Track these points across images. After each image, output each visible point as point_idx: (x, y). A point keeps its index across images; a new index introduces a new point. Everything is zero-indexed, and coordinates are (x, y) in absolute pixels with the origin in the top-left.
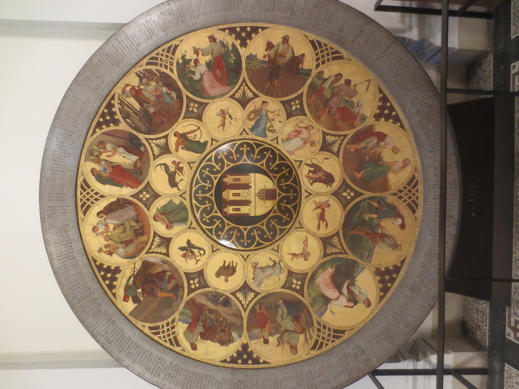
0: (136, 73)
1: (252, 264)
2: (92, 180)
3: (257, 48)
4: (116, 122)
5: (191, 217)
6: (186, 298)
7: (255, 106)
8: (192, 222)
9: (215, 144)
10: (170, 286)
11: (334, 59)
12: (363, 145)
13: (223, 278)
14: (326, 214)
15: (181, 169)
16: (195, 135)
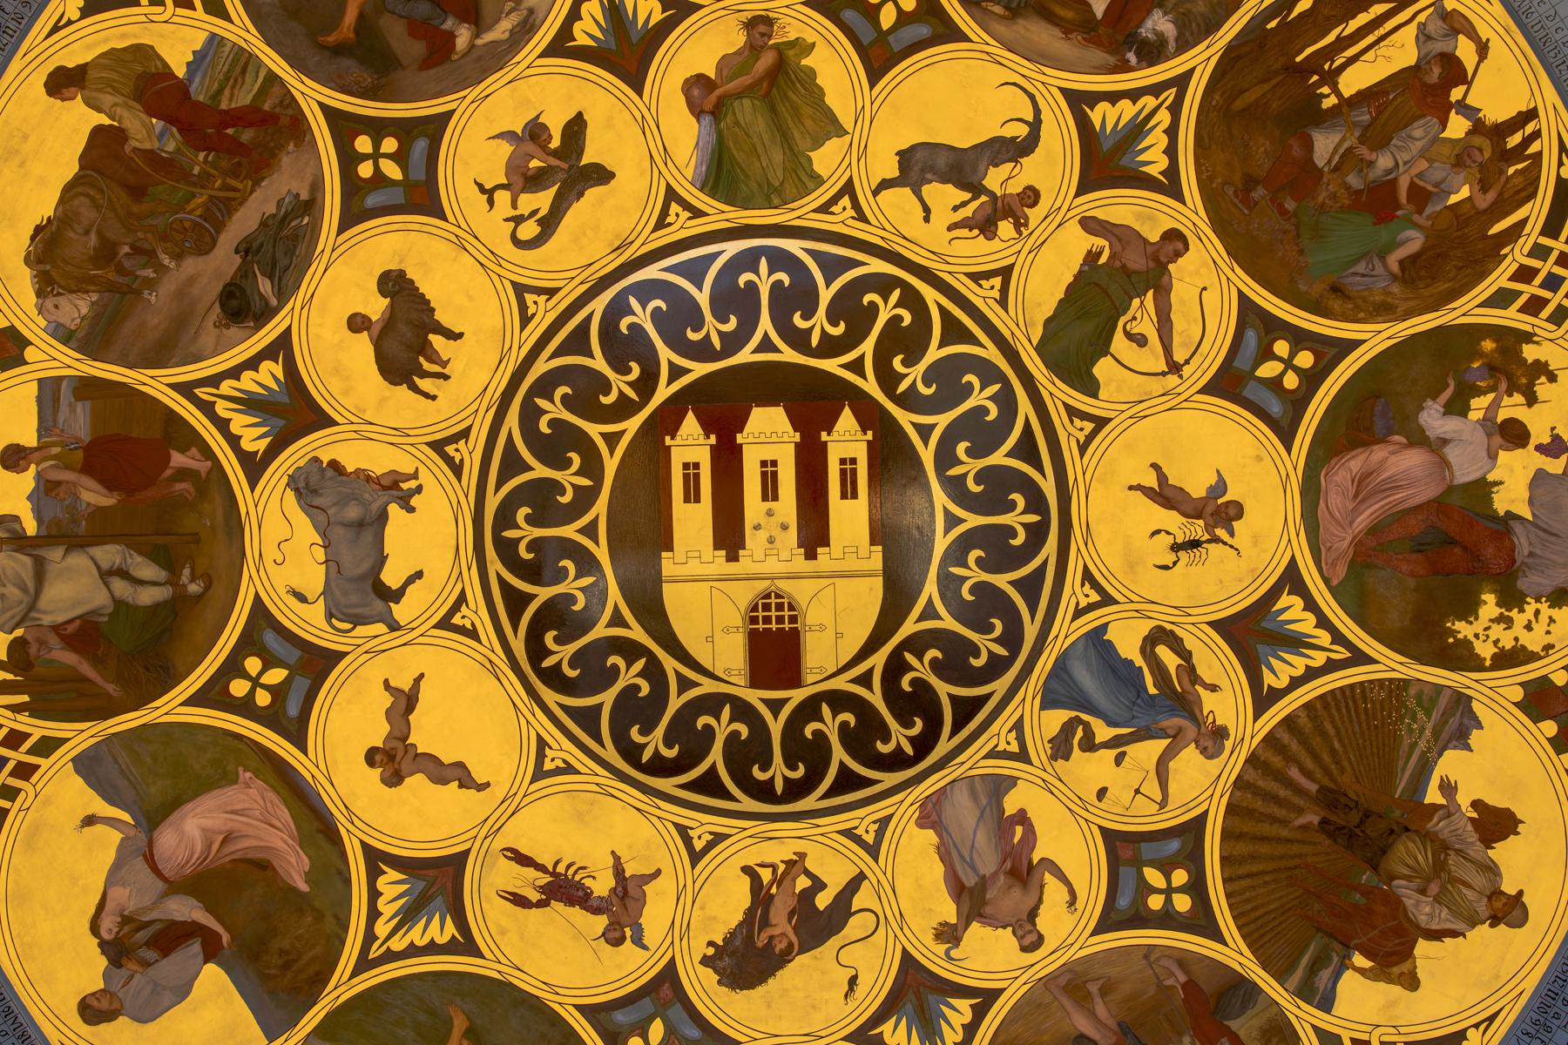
0: (1531, 114)
1: (415, 476)
5: (720, 215)
6: (311, 96)
7: (1213, 688)
9: (1069, 433)
13: (376, 307)
14: (576, 913)
15: (986, 226)
16: (1141, 341)
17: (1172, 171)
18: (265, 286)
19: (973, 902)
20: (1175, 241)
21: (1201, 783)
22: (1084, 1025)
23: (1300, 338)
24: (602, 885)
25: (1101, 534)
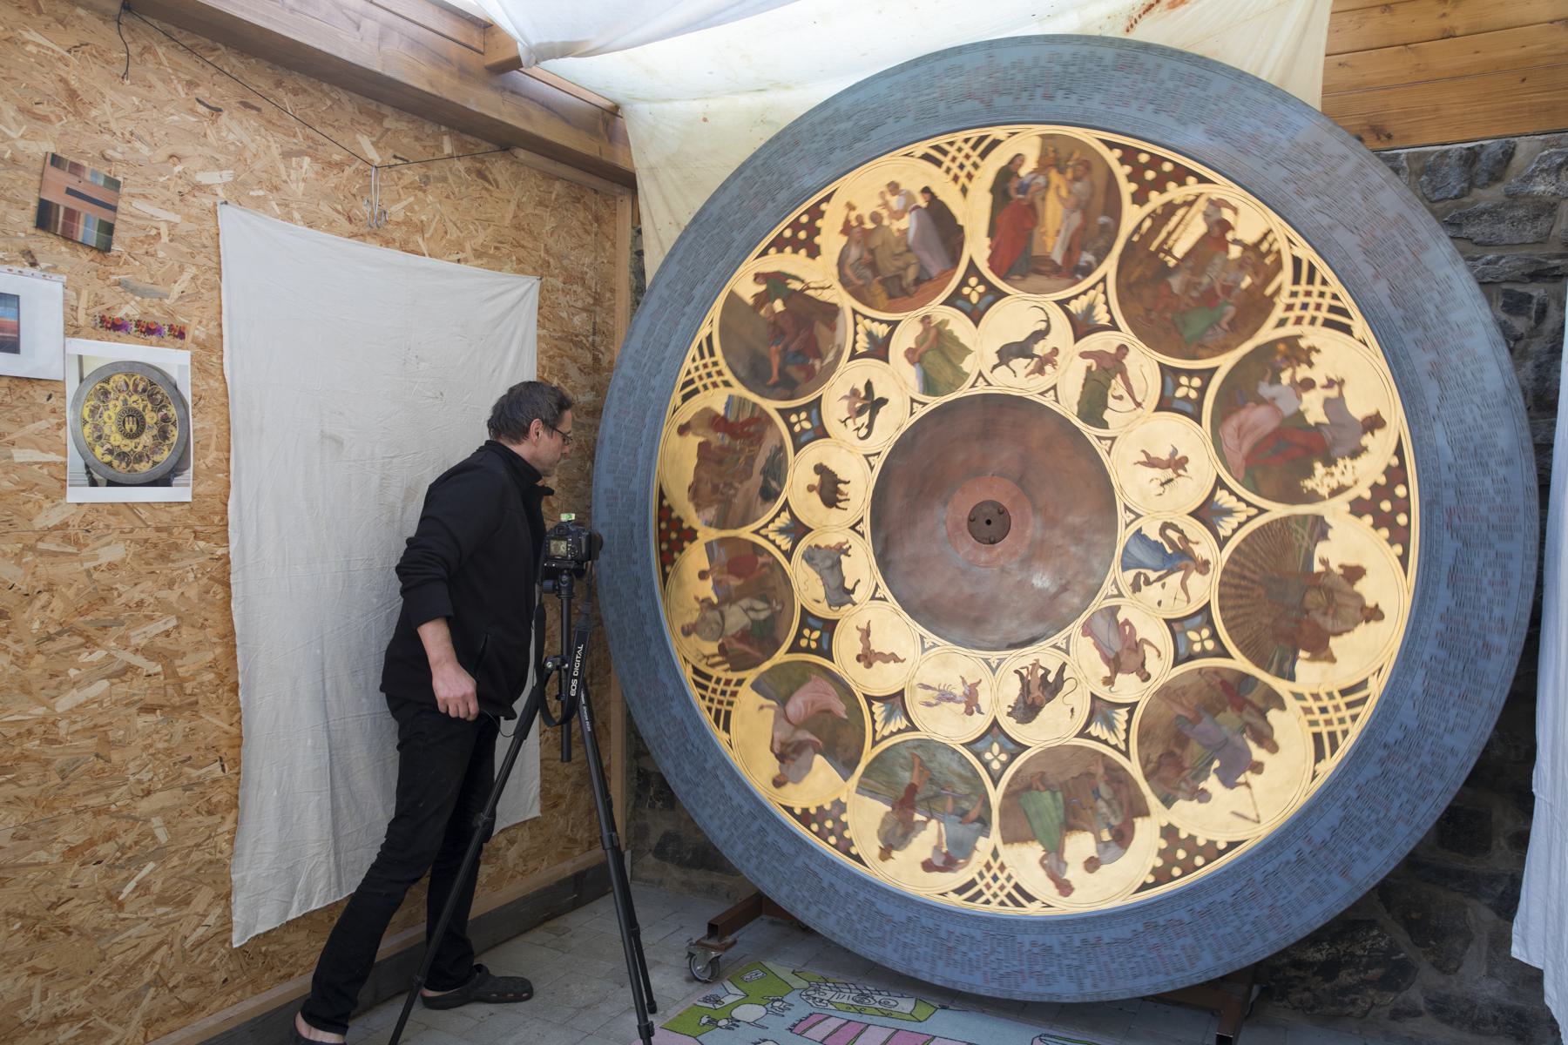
0: (1270, 231)
2: (998, 159)
3: (1349, 542)
4: (1139, 199)
6: (770, 406)
8: (925, 404)
9: (1101, 448)
10: (792, 370)
11: (1317, 738)
12: (1105, 791)
13: (816, 479)
14: (952, 704)
16: (1120, 398)
17: (1112, 320)
18: (774, 484)
19: (1116, 664)
20: (1123, 350)
21: (1204, 589)
22: (1180, 711)
23: (1190, 373)
24: (959, 690)
25: (1128, 489)
